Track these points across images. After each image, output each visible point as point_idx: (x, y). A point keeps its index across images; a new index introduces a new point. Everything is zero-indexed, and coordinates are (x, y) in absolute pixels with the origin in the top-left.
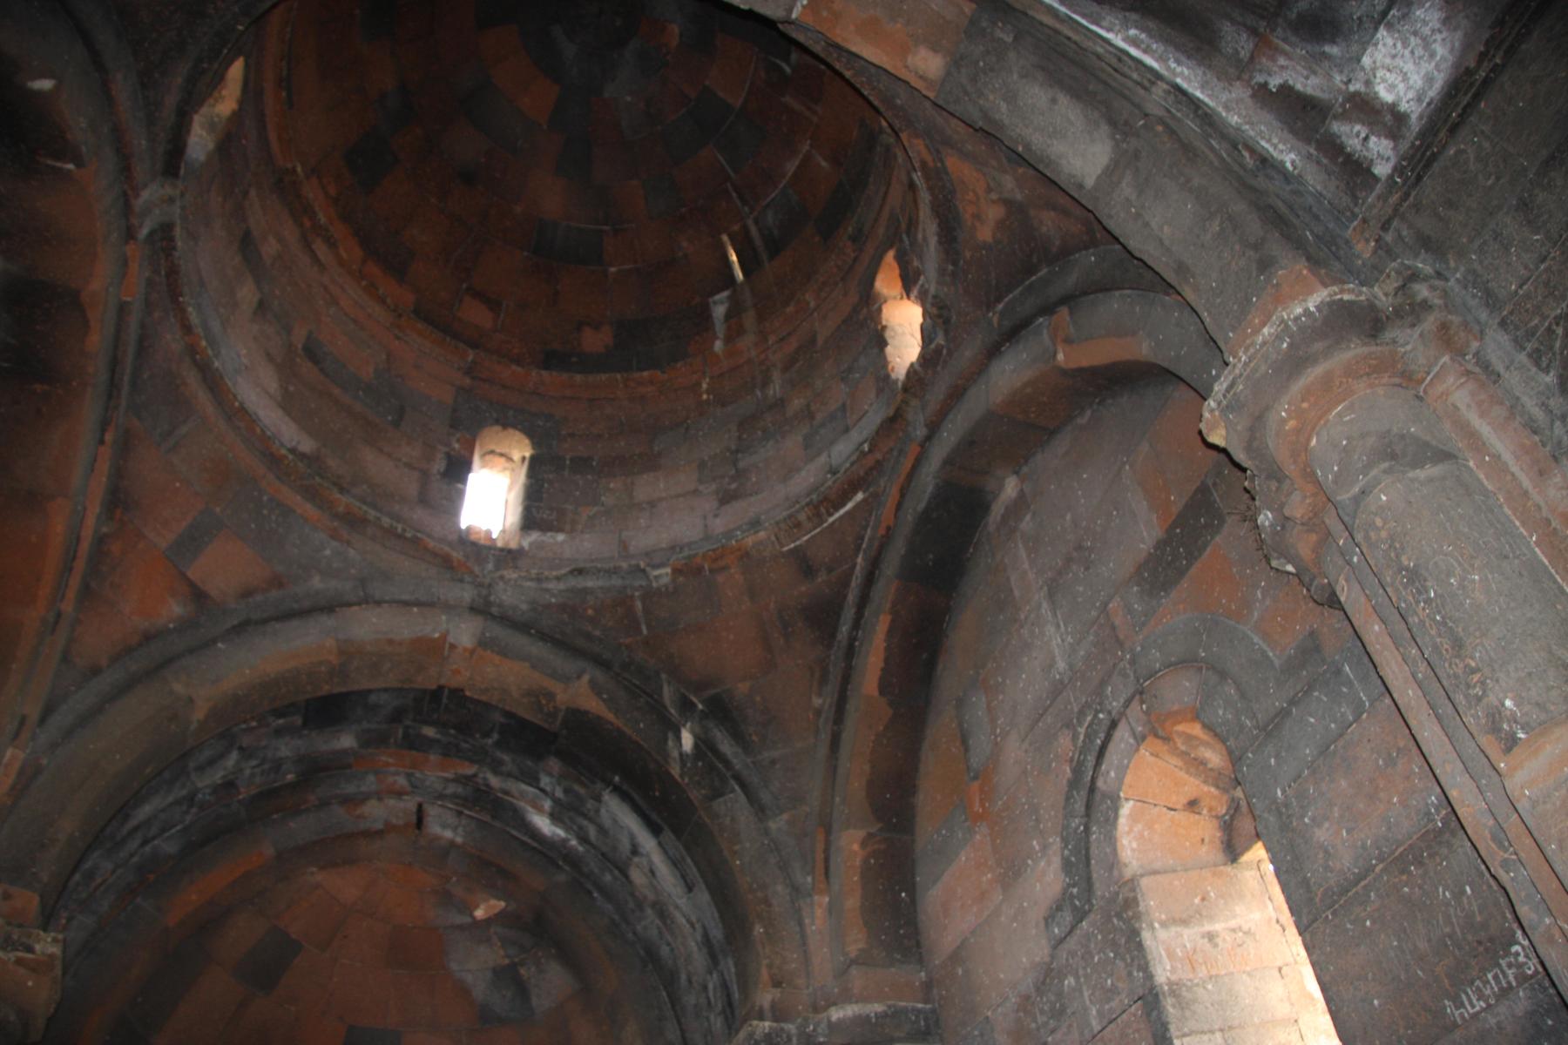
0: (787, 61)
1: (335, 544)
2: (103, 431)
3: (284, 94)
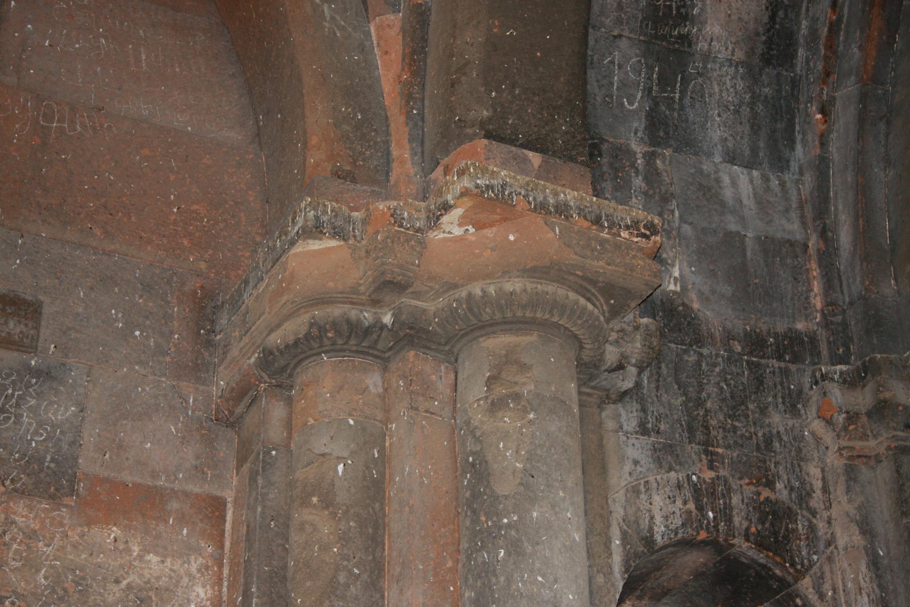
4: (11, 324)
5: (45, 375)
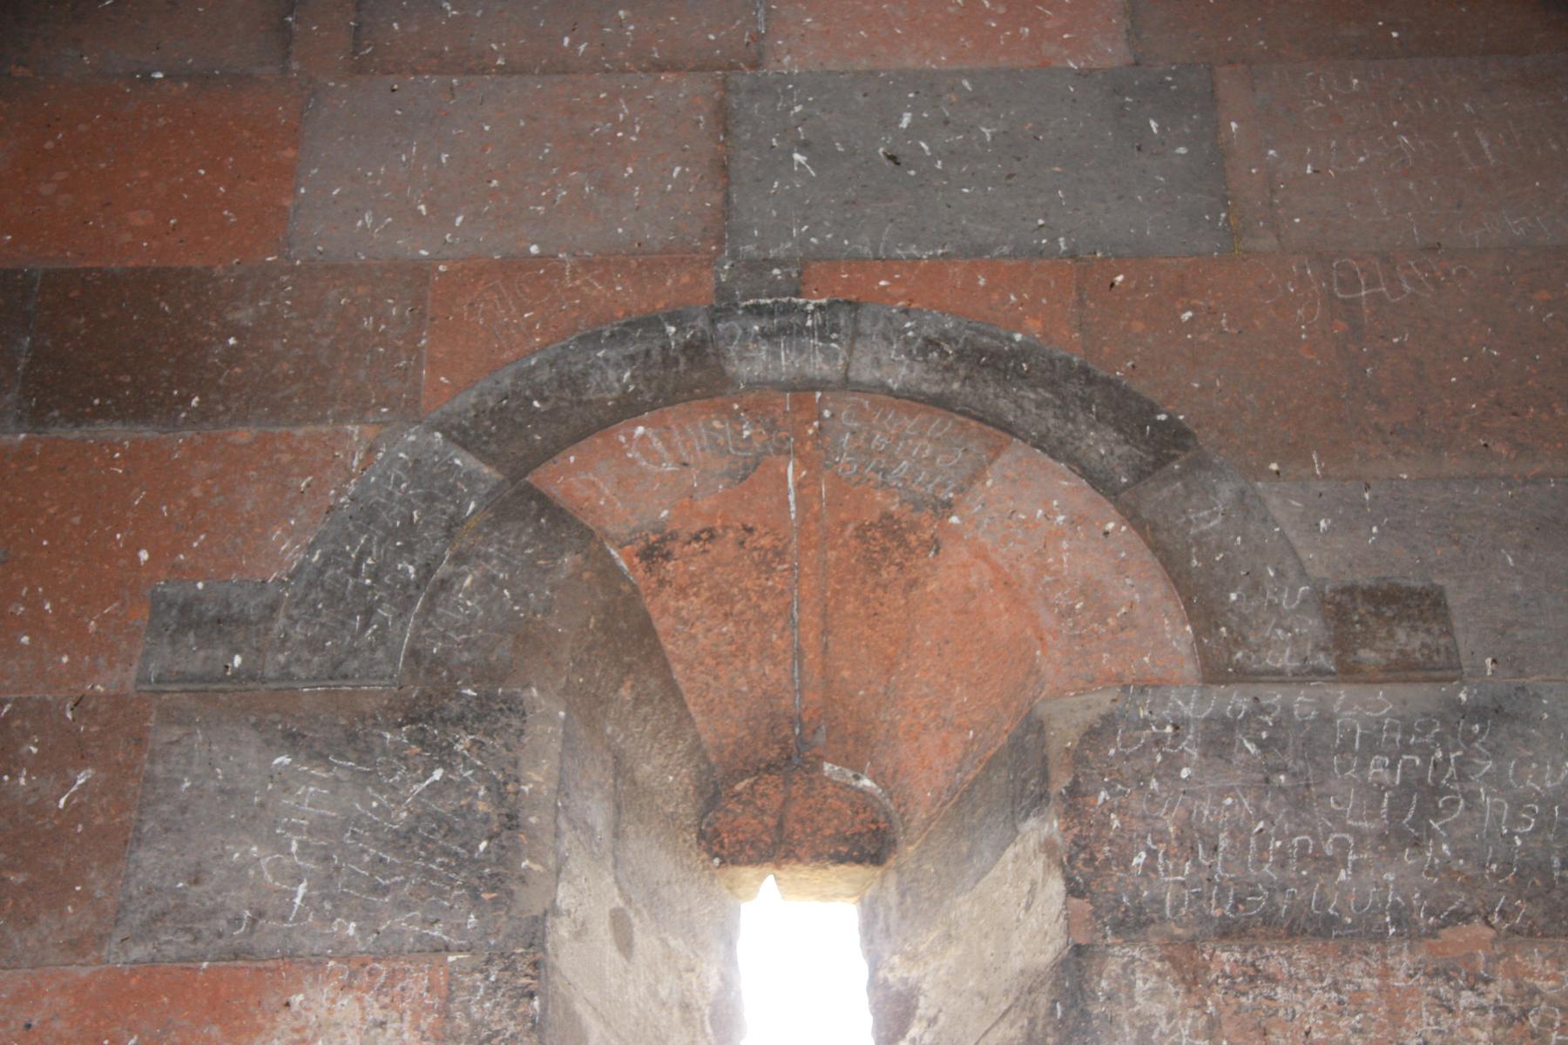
4: (1401, 635)
5: (1492, 712)
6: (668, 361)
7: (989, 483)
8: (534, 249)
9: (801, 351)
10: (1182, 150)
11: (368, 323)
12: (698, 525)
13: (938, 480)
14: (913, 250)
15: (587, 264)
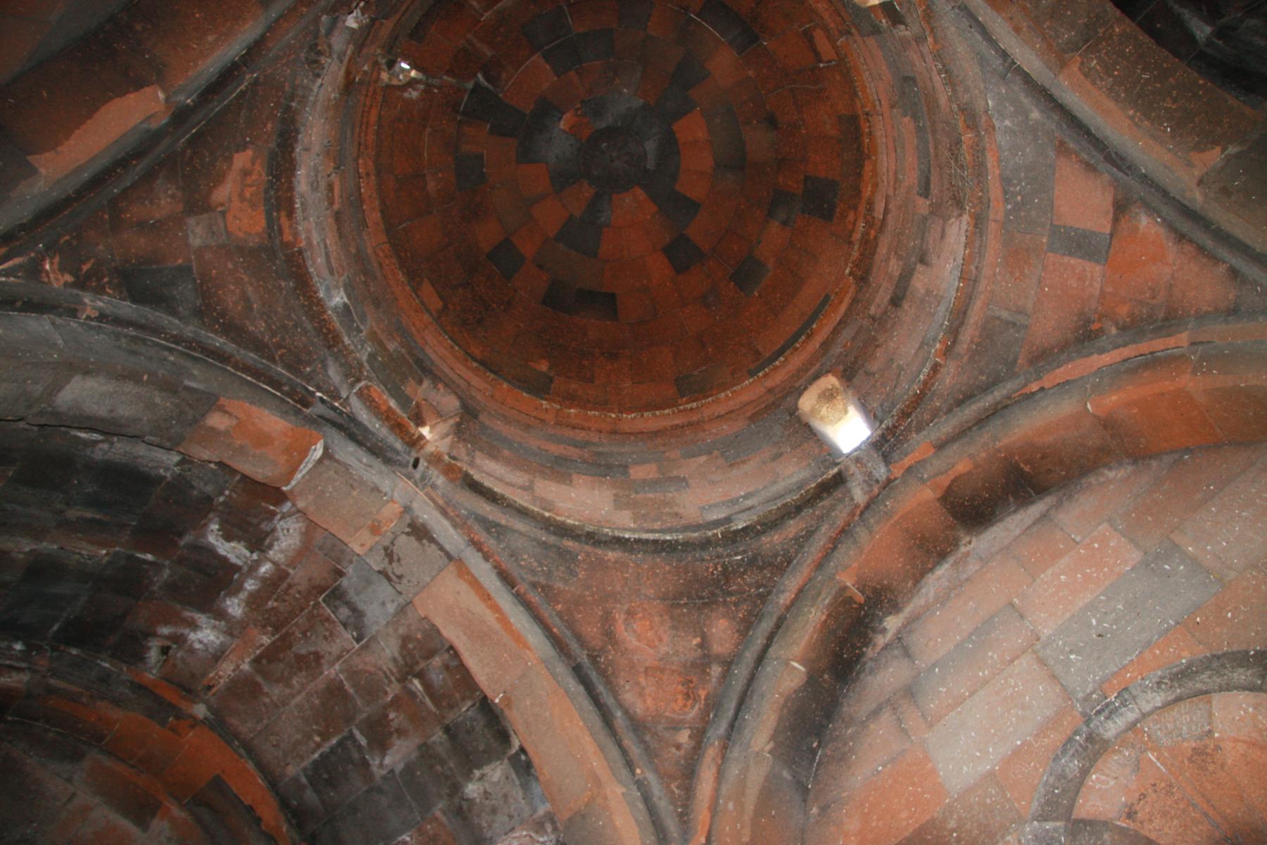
0: (477, 85)
1: (997, 124)
2: (1033, 394)
3: (814, 326)
6: (1085, 749)
7: (1217, 714)
8: (1019, 743)
9: (1122, 715)
10: (1182, 567)
11: (988, 801)
12: (1137, 795)
13: (1199, 725)
14: (1129, 658)
15: (1037, 736)
